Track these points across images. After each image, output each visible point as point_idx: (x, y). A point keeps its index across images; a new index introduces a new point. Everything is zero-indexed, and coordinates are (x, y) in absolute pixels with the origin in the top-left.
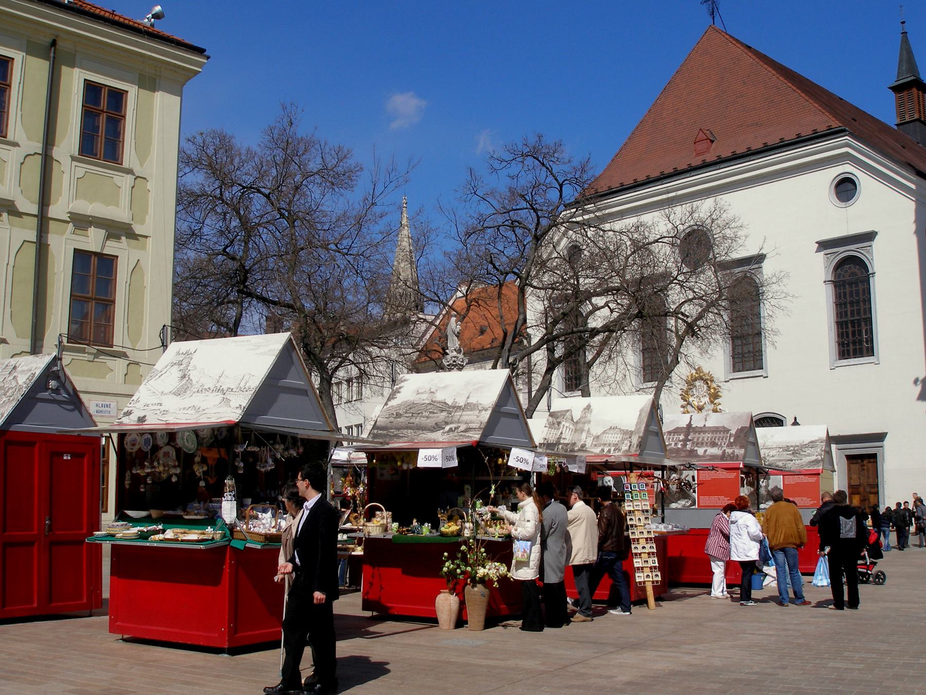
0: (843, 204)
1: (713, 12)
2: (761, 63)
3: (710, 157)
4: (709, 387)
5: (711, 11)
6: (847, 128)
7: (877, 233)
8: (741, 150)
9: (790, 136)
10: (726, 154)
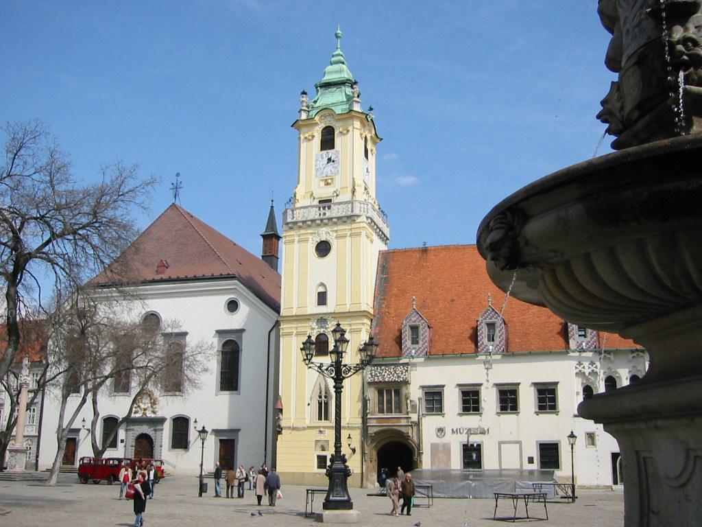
0: (231, 313)
3: (165, 277)
4: (151, 400)
10: (174, 277)
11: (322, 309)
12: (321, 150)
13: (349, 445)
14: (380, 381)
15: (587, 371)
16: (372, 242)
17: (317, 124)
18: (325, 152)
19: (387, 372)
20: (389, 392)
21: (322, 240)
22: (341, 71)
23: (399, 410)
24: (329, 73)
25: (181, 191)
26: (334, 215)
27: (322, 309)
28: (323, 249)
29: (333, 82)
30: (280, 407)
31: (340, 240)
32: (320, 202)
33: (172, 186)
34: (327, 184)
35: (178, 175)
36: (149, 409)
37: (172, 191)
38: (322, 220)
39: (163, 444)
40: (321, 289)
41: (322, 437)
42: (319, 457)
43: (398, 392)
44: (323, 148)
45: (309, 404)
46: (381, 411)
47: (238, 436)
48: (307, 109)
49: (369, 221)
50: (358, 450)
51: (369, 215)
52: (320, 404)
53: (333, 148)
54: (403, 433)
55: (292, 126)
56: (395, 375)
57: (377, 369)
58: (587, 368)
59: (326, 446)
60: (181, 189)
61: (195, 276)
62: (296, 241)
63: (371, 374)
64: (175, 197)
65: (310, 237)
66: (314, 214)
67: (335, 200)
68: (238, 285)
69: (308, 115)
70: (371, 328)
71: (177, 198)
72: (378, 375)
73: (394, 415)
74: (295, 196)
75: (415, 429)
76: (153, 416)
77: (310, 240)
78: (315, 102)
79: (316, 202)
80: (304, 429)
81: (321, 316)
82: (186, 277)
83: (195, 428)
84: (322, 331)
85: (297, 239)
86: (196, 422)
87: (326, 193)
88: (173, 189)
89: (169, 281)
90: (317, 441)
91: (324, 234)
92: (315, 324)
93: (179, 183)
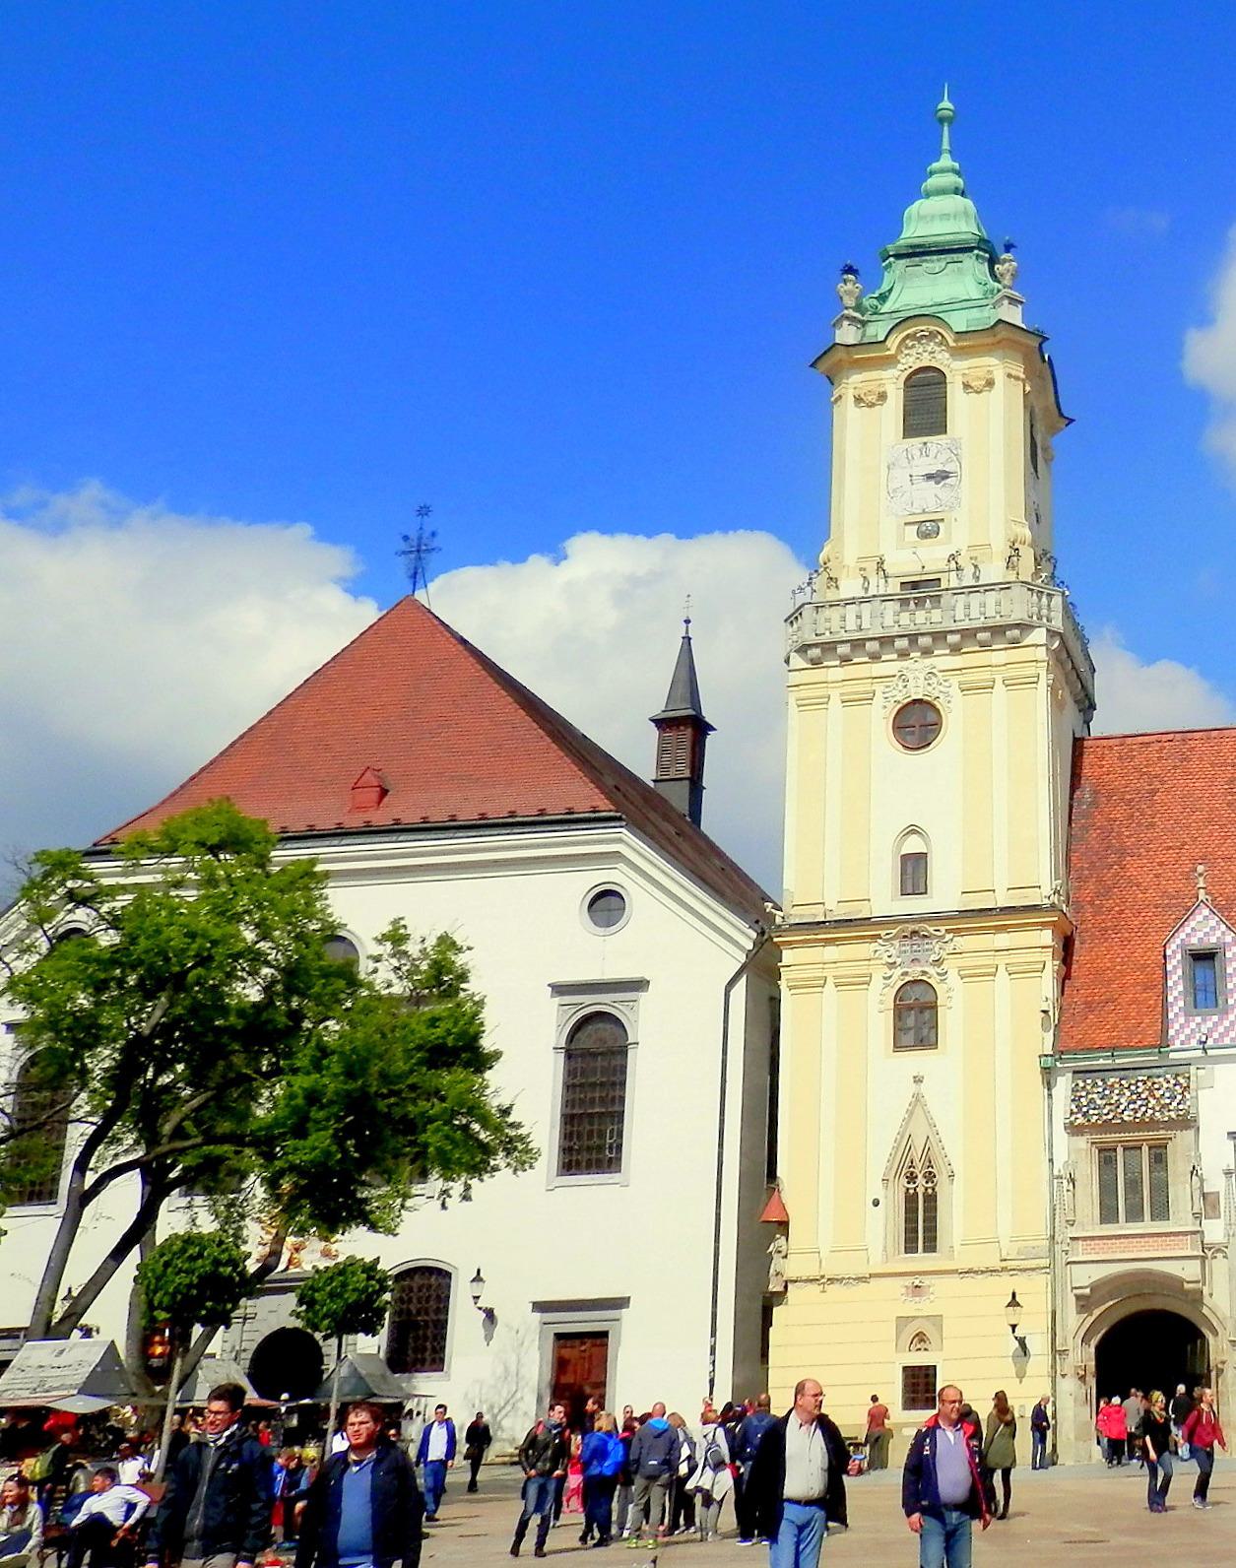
1: (415, 573)
2: (490, 680)
5: (412, 572)
6: (624, 817)
7: (648, 982)
8: (438, 816)
9: (527, 810)
31: (973, 699)
33: (403, 546)
34: (924, 535)
35: (424, 511)
37: (402, 559)
38: (913, 638)
40: (914, 845)
43: (1159, 1157)
46: (1108, 1214)
54: (1182, 1281)
56: (1153, 1102)
57: (1095, 1085)
60: (434, 556)
62: (835, 701)
64: (414, 576)
65: (879, 688)
66: (891, 619)
67: (951, 581)
72: (1099, 1102)
73: (1147, 1226)
75: (1219, 1266)
79: (894, 587)
81: (912, 927)
84: (915, 972)
87: (930, 558)
91: (916, 677)
93: (426, 534)
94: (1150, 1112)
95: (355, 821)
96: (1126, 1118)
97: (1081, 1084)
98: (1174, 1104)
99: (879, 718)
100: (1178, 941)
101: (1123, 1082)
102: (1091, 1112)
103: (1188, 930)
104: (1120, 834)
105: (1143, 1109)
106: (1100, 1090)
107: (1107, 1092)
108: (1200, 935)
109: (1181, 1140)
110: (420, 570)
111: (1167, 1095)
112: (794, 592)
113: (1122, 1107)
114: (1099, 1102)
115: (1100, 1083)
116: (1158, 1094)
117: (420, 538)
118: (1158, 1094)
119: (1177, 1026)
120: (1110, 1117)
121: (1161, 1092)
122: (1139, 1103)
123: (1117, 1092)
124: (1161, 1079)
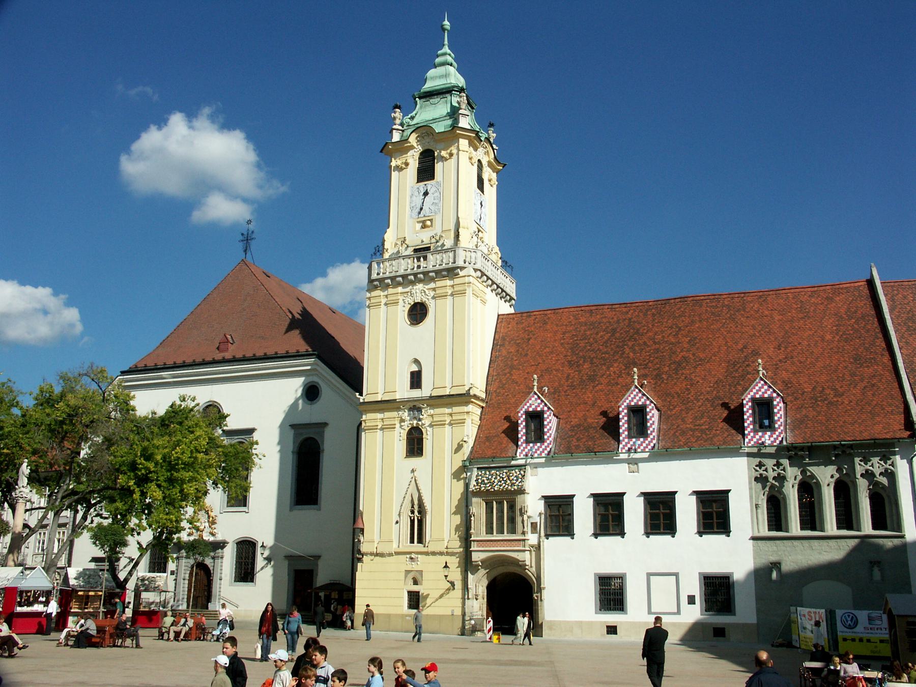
0: (309, 402)
3: (228, 355)
4: (209, 517)
10: (239, 355)
11: (416, 394)
12: (418, 182)
13: (446, 576)
14: (488, 490)
15: (771, 474)
16: (484, 302)
17: (412, 147)
18: (422, 184)
19: (499, 478)
20: (500, 503)
21: (416, 301)
22: (446, 76)
23: (513, 531)
24: (432, 78)
25: (253, 243)
26: (430, 268)
27: (416, 394)
28: (418, 313)
29: (436, 90)
30: (361, 526)
32: (416, 251)
33: (241, 238)
34: (424, 226)
36: (206, 530)
37: (241, 244)
38: (415, 275)
39: (223, 576)
40: (415, 368)
41: (414, 567)
42: (410, 593)
44: (420, 180)
45: (397, 522)
46: (489, 530)
47: (317, 565)
48: (400, 128)
49: (479, 274)
50: (459, 585)
51: (478, 266)
52: (412, 522)
53: (433, 178)
55: (381, 151)
56: (509, 482)
57: (485, 474)
58: (770, 470)
59: (418, 577)
60: (253, 241)
61: (265, 354)
63: (477, 480)
65: (401, 298)
68: (318, 365)
69: (402, 136)
70: (480, 420)
71: (249, 254)
73: (506, 536)
74: (383, 245)
76: (212, 539)
77: (401, 302)
78: (412, 118)
79: (410, 251)
80: (390, 555)
82: (254, 355)
83: (262, 554)
85: (384, 301)
86: (262, 546)
87: (425, 237)
88: (242, 241)
89: (234, 360)
90: (408, 572)
92: (406, 414)
94: (507, 486)
95: (219, 356)
96: (496, 489)
97: (480, 473)
98: (517, 483)
99: (402, 311)
100: (524, 410)
101: (498, 473)
102: (482, 486)
103: (528, 404)
104: (512, 359)
105: (504, 485)
106: (487, 476)
107: (490, 477)
108: (533, 407)
109: (519, 498)
110: (248, 248)
111: (515, 479)
112: (372, 255)
113: (495, 484)
114: (486, 481)
115: (488, 473)
116: (511, 478)
117: (248, 234)
118: (511, 478)
119: (522, 448)
120: (489, 488)
121: (513, 477)
122: (503, 482)
123: (494, 477)
124: (514, 472)
